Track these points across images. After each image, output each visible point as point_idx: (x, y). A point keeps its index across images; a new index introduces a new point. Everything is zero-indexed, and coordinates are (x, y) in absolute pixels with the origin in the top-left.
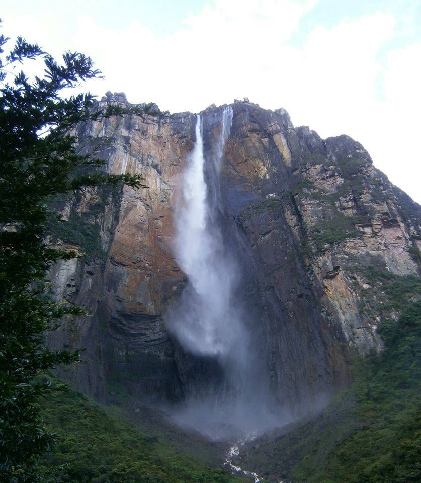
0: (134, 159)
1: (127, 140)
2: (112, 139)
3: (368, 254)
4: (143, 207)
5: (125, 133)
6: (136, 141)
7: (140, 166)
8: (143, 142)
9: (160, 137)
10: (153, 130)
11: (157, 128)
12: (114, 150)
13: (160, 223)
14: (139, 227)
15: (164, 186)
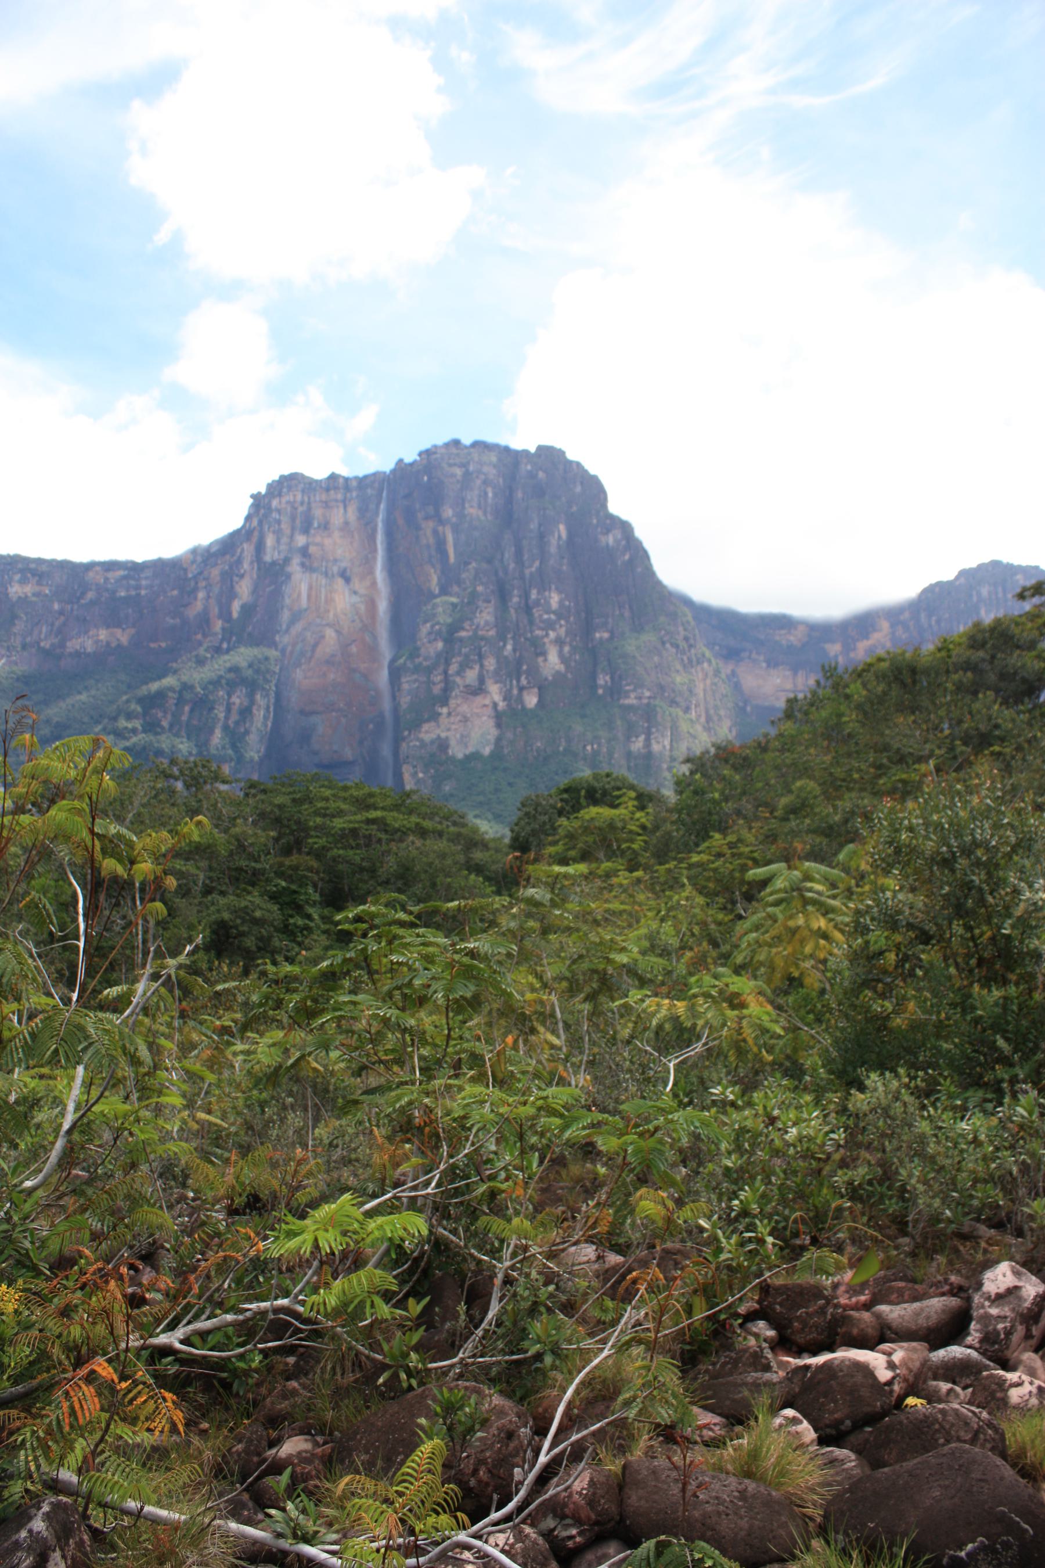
0: (314, 576)
1: (304, 551)
2: (287, 561)
3: (439, 737)
4: (333, 634)
5: (301, 540)
6: (317, 544)
7: (324, 581)
8: (327, 542)
9: (346, 523)
10: (337, 517)
11: (342, 510)
12: (289, 576)
13: (354, 649)
14: (329, 662)
15: (355, 599)
